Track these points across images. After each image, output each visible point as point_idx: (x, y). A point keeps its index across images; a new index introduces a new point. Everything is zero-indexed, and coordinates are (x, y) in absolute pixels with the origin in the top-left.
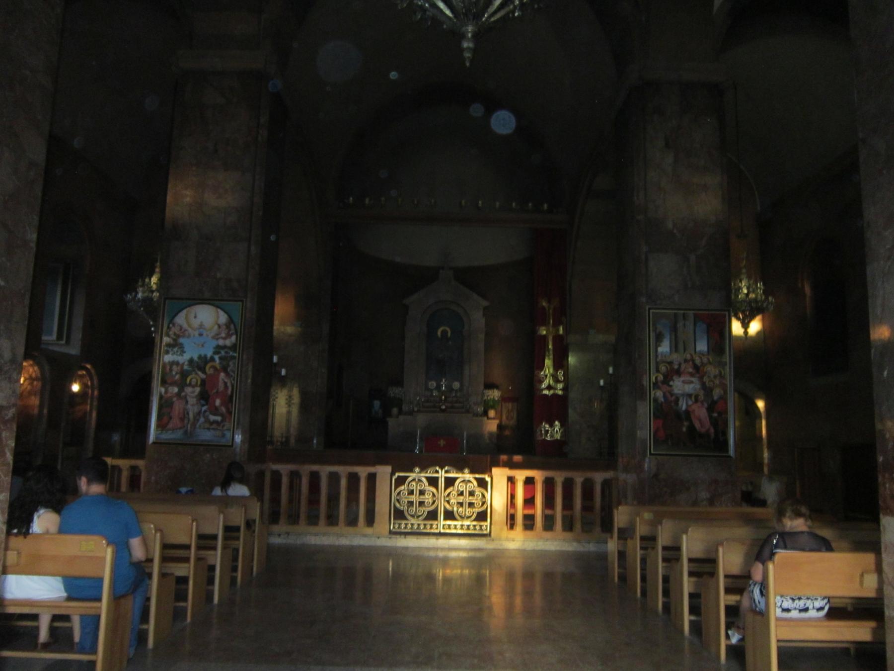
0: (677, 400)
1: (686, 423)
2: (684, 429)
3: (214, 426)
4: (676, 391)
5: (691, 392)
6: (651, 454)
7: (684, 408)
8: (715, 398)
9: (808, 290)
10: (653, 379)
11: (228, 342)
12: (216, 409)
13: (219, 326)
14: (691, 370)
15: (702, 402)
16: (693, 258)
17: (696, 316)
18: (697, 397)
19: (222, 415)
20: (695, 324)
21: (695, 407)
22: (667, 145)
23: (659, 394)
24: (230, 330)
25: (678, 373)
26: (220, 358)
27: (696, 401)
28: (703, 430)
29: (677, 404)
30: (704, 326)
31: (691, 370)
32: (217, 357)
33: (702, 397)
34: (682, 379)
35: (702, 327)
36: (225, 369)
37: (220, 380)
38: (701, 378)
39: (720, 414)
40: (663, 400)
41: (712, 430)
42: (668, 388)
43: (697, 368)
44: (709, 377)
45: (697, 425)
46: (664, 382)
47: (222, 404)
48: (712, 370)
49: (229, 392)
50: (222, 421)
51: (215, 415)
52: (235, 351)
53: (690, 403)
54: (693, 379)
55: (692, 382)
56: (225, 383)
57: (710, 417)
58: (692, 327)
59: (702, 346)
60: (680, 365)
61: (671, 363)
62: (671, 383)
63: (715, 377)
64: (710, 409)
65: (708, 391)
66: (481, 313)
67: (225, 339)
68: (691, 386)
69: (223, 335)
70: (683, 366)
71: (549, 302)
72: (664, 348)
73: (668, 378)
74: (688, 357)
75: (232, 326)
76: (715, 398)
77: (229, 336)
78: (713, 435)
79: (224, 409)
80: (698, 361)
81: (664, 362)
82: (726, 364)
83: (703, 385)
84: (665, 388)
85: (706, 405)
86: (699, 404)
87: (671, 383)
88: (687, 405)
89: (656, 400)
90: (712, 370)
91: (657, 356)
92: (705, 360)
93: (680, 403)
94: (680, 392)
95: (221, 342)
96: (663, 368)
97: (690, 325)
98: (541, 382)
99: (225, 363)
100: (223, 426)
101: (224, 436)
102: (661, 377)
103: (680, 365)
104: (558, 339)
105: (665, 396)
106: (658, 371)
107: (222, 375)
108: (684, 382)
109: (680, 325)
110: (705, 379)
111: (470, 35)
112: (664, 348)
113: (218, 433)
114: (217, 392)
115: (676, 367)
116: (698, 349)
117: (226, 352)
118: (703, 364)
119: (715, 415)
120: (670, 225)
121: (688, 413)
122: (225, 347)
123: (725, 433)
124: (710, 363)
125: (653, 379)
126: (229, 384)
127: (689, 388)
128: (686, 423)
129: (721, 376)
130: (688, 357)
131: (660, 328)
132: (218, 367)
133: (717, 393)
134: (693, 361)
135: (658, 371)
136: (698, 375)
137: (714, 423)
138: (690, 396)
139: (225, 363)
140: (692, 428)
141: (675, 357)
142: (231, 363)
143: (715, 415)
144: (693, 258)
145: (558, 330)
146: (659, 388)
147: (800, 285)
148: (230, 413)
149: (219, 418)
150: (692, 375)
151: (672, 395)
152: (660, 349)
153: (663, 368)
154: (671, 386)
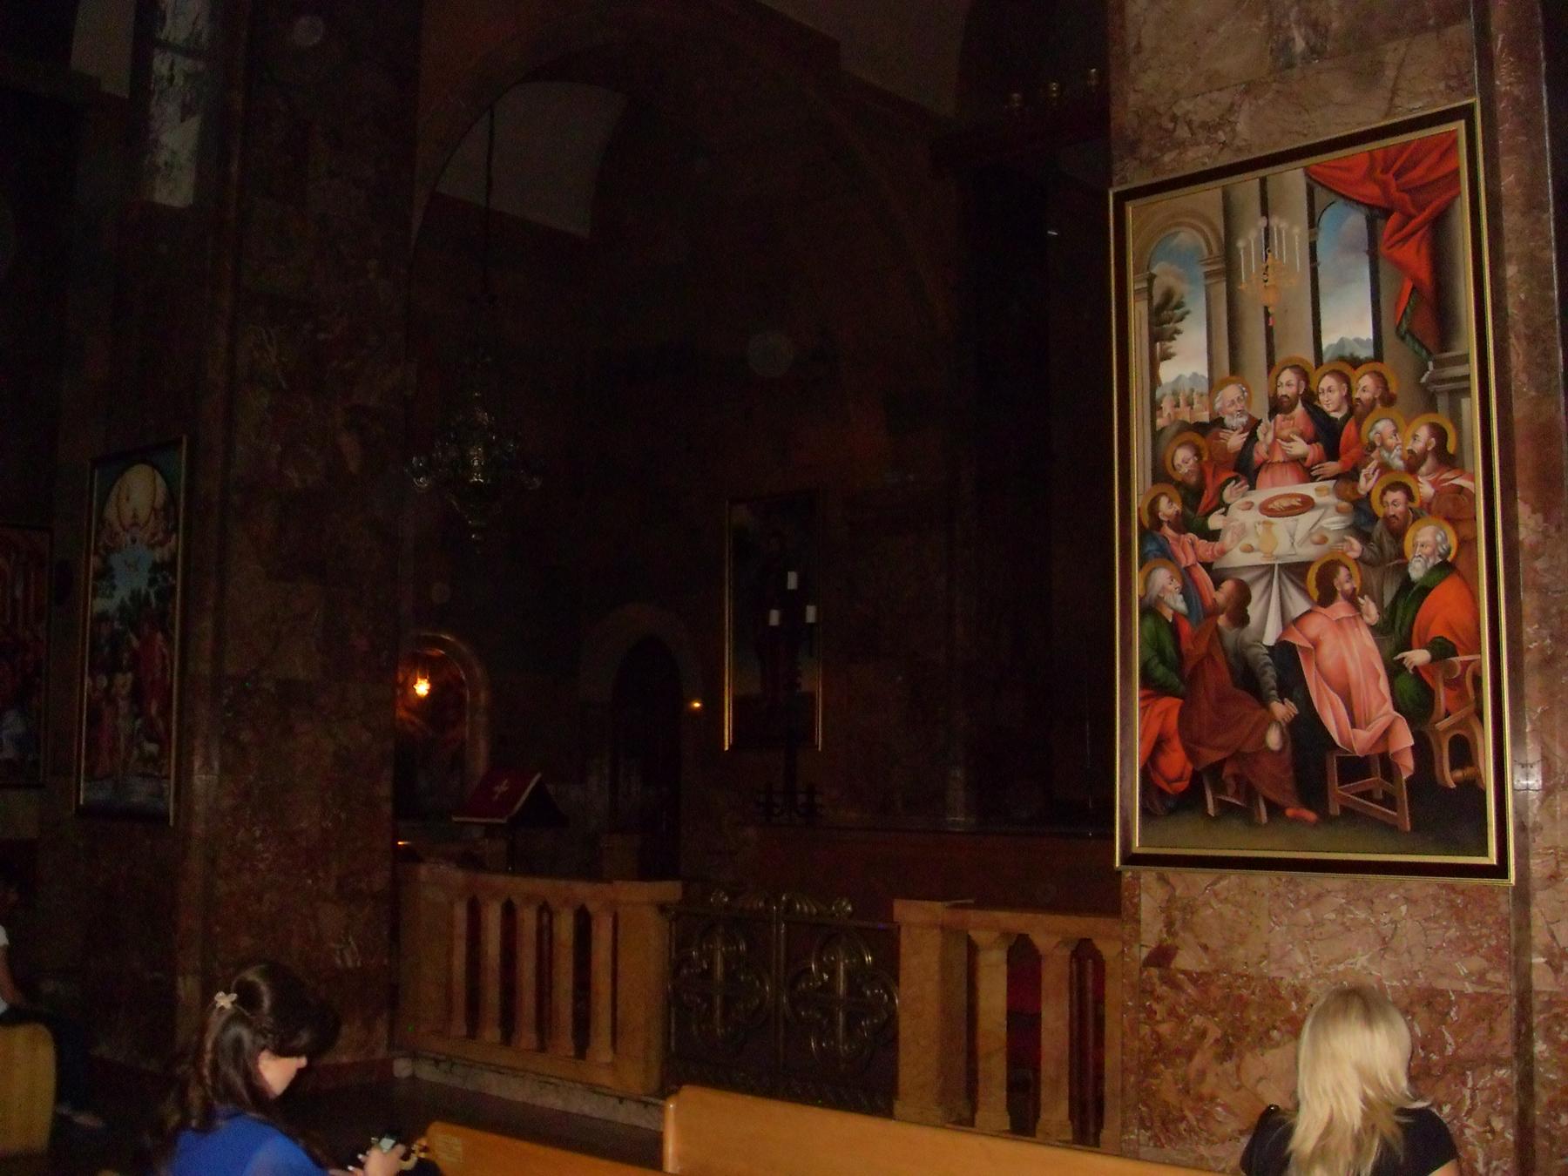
1: (1283, 710)
2: (1274, 739)
4: (1237, 558)
5: (1307, 552)
7: (1270, 638)
8: (1417, 571)
14: (1299, 447)
15: (1352, 599)
17: (1314, 183)
20: (1313, 223)
25: (1246, 469)
28: (1361, 740)
29: (1241, 619)
30: (1356, 221)
31: (1299, 447)
33: (1345, 581)
34: (1258, 497)
39: (1442, 650)
40: (1181, 606)
41: (1404, 739)
42: (1202, 544)
43: (1327, 433)
44: (1384, 468)
45: (1333, 717)
46: (1183, 524)
48: (1397, 436)
54: (1309, 489)
55: (1307, 504)
57: (1395, 670)
58: (1299, 231)
59: (1349, 322)
60: (1252, 427)
62: (1215, 522)
64: (1394, 632)
68: (1306, 520)
70: (1265, 435)
78: (1407, 765)
80: (1331, 397)
81: (1185, 427)
83: (1362, 517)
84: (1189, 549)
85: (1372, 612)
86: (1340, 609)
87: (1215, 522)
88: (1289, 623)
89: (1151, 610)
90: (1397, 436)
91: (1155, 407)
93: (1254, 611)
94: (1256, 559)
97: (1291, 228)
102: (1168, 508)
103: (1252, 427)
105: (1189, 588)
106: (1161, 474)
108: (1266, 509)
109: (1249, 241)
110: (1364, 485)
115: (1235, 441)
118: (1356, 411)
119: (1418, 657)
121: (1285, 654)
124: (1388, 400)
127: (1292, 539)
128: (1283, 710)
129: (1447, 459)
131: (1165, 273)
133: (1426, 543)
134: (1309, 399)
136: (1332, 467)
138: (1296, 571)
140: (1307, 728)
143: (1418, 657)
150: (1307, 473)
152: (1167, 372)
153: (1183, 459)
154: (1214, 536)
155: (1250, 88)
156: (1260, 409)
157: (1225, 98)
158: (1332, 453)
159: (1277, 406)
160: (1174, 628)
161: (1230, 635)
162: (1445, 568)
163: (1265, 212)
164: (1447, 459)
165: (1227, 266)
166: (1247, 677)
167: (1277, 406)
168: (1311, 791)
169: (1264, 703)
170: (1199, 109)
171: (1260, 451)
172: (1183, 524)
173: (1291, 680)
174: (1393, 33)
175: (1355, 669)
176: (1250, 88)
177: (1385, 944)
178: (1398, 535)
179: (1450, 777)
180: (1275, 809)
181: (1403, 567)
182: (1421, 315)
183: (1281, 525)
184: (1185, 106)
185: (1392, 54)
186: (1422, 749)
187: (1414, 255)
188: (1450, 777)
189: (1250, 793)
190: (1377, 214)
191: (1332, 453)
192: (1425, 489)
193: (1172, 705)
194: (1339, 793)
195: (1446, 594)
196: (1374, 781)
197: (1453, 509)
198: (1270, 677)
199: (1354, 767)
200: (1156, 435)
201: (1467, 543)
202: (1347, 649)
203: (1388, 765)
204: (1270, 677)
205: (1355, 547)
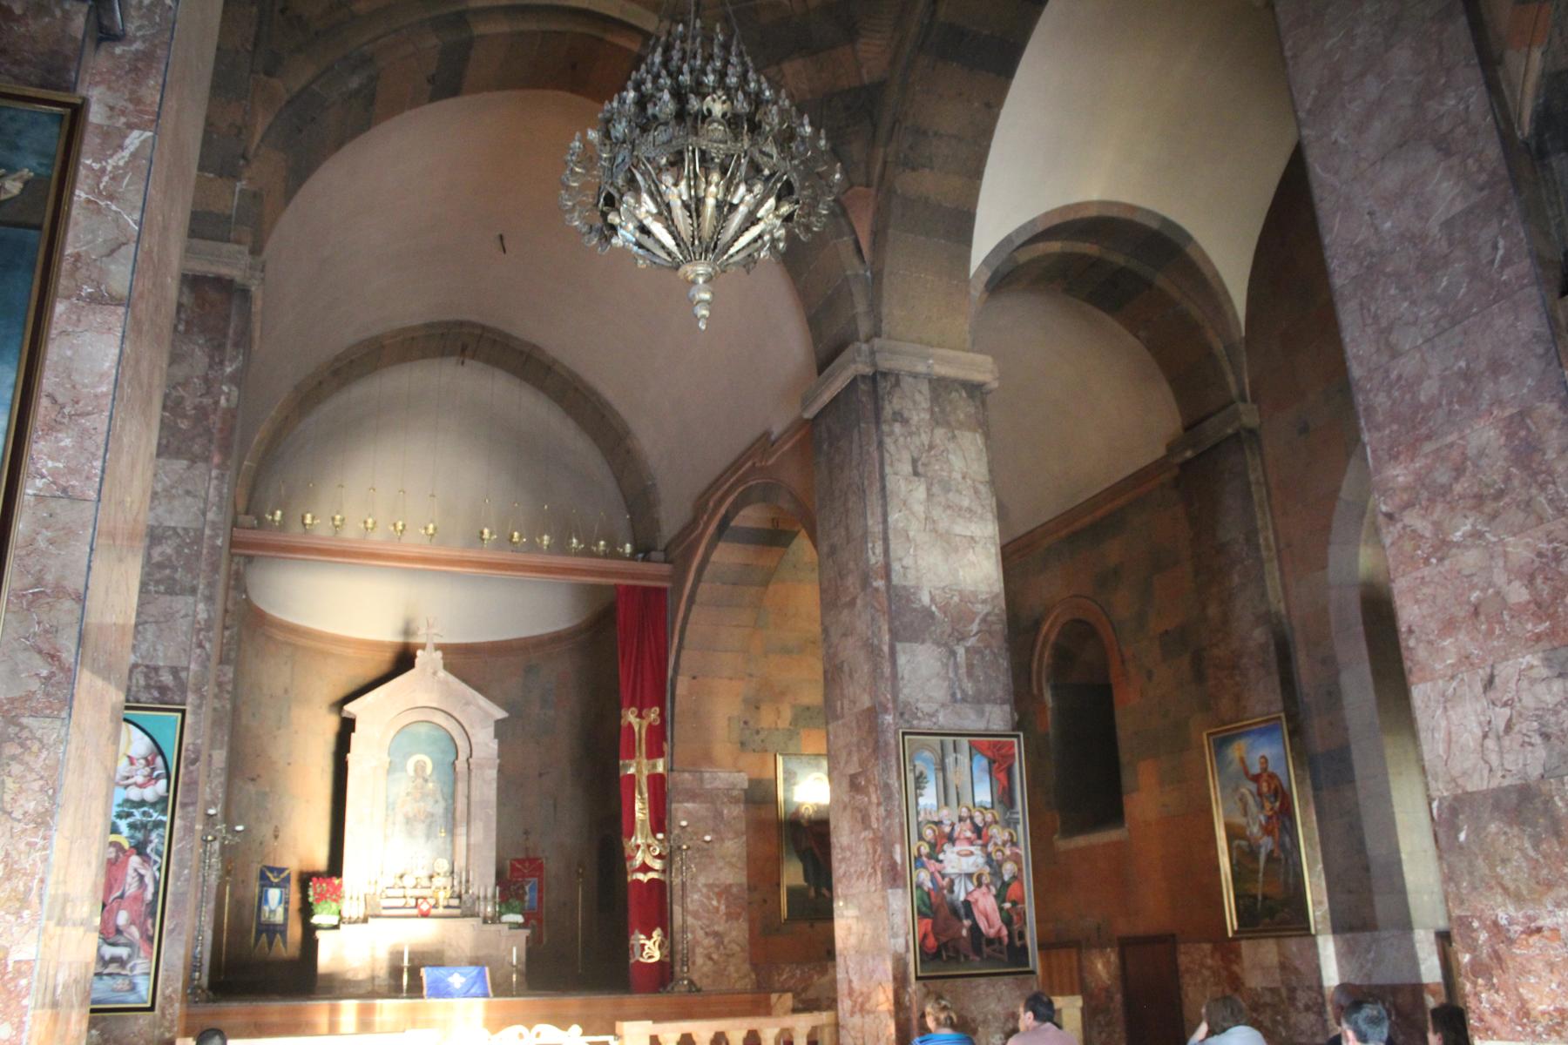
0: (952, 882)
1: (967, 923)
2: (964, 932)
3: (113, 968)
4: (949, 870)
5: (972, 870)
6: (918, 978)
7: (962, 898)
8: (1006, 878)
9: (1048, 696)
10: (914, 852)
11: (150, 794)
12: (119, 931)
13: (131, 760)
14: (969, 834)
16: (961, 651)
17: (972, 746)
18: (979, 877)
19: (129, 944)
21: (977, 894)
22: (916, 473)
23: (924, 876)
24: (153, 770)
25: (951, 839)
26: (132, 826)
27: (980, 885)
28: (992, 932)
29: (951, 891)
30: (985, 762)
31: (969, 834)
32: (123, 824)
33: (986, 879)
34: (957, 849)
35: (981, 763)
36: (140, 848)
37: (130, 871)
38: (985, 846)
39: (1014, 903)
41: (1005, 932)
43: (978, 831)
45: (983, 925)
46: (930, 856)
47: (132, 922)
48: (999, 834)
49: (149, 896)
50: (130, 956)
51: (114, 944)
52: (164, 812)
53: (971, 888)
54: (972, 848)
55: (972, 853)
56: (141, 877)
57: (1001, 909)
59: (983, 795)
60: (953, 825)
61: (939, 823)
62: (941, 857)
63: (1004, 844)
64: (1000, 897)
65: (995, 866)
66: (491, 730)
67: (141, 786)
68: (971, 859)
69: (140, 779)
70: (957, 829)
71: (640, 716)
72: (929, 799)
73: (935, 849)
74: (964, 812)
75: (159, 760)
76: (1006, 878)
77: (151, 779)
78: (1006, 940)
79: (135, 932)
80: (978, 820)
82: (1017, 822)
83: (989, 860)
85: (993, 890)
86: (984, 889)
88: (968, 894)
89: (919, 886)
90: (999, 834)
91: (918, 813)
92: (989, 817)
93: (956, 888)
94: (956, 871)
95: (134, 793)
96: (928, 833)
97: (964, 758)
98: (632, 858)
99: (139, 835)
100: (132, 969)
101: (133, 988)
102: (925, 849)
103: (953, 825)
104: (657, 782)
105: (933, 879)
106: (921, 838)
107: (135, 860)
108: (958, 853)
109: (950, 760)
110: (990, 848)
111: (701, 280)
112: (929, 799)
113: (120, 983)
114: (122, 897)
115: (947, 829)
116: (977, 800)
117: (144, 813)
119: (1007, 905)
120: (926, 600)
121: (967, 904)
122: (142, 803)
123: (1022, 936)
124: (996, 822)
125: (914, 852)
126: (149, 880)
128: (967, 923)
129: (1014, 844)
130: (964, 812)
132: (126, 846)
133: (1008, 869)
134: (972, 818)
135: (921, 838)
137: (1008, 921)
138: (969, 876)
139: (139, 835)
140: (975, 928)
141: (947, 815)
142: (154, 836)
143: (1007, 905)
144: (961, 651)
145: (654, 766)
146: (923, 866)
147: (1035, 691)
148: (151, 939)
149: (123, 952)
150: (971, 842)
151: (943, 876)
152: (922, 801)
153: (928, 833)
155: (943, 705)
156: (956, 820)
157: (935, 706)
158: (979, 837)
159: (961, 819)
160: (928, 894)
161: (948, 897)
162: (1014, 878)
163: (955, 750)
164: (1014, 844)
165: (943, 768)
166: (954, 911)
167: (961, 819)
168: (978, 951)
169: (960, 920)
170: (926, 707)
171: (956, 834)
172: (930, 856)
173: (969, 914)
174: (988, 701)
175: (989, 909)
176: (943, 705)
177: (999, 1000)
178: (1000, 866)
179: (1018, 943)
180: (966, 957)
181: (1002, 877)
182: (1005, 798)
183: (964, 859)
184: (920, 705)
185: (988, 708)
186: (1010, 935)
187: (1002, 776)
188: (1018, 943)
189: (957, 951)
190: (991, 762)
191: (979, 837)
192: (1008, 852)
193: (929, 921)
194: (986, 950)
195: (1014, 885)
196: (996, 946)
197: (1016, 859)
198: (962, 911)
199: (990, 942)
200: (919, 824)
201: (1020, 870)
202: (986, 903)
203: (1000, 939)
204: (962, 911)
205: (987, 869)
